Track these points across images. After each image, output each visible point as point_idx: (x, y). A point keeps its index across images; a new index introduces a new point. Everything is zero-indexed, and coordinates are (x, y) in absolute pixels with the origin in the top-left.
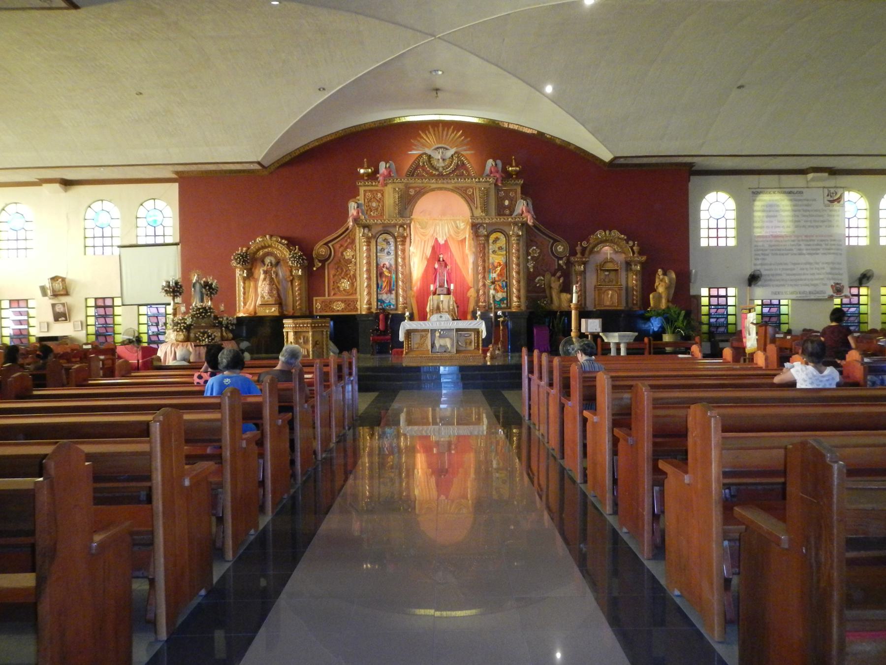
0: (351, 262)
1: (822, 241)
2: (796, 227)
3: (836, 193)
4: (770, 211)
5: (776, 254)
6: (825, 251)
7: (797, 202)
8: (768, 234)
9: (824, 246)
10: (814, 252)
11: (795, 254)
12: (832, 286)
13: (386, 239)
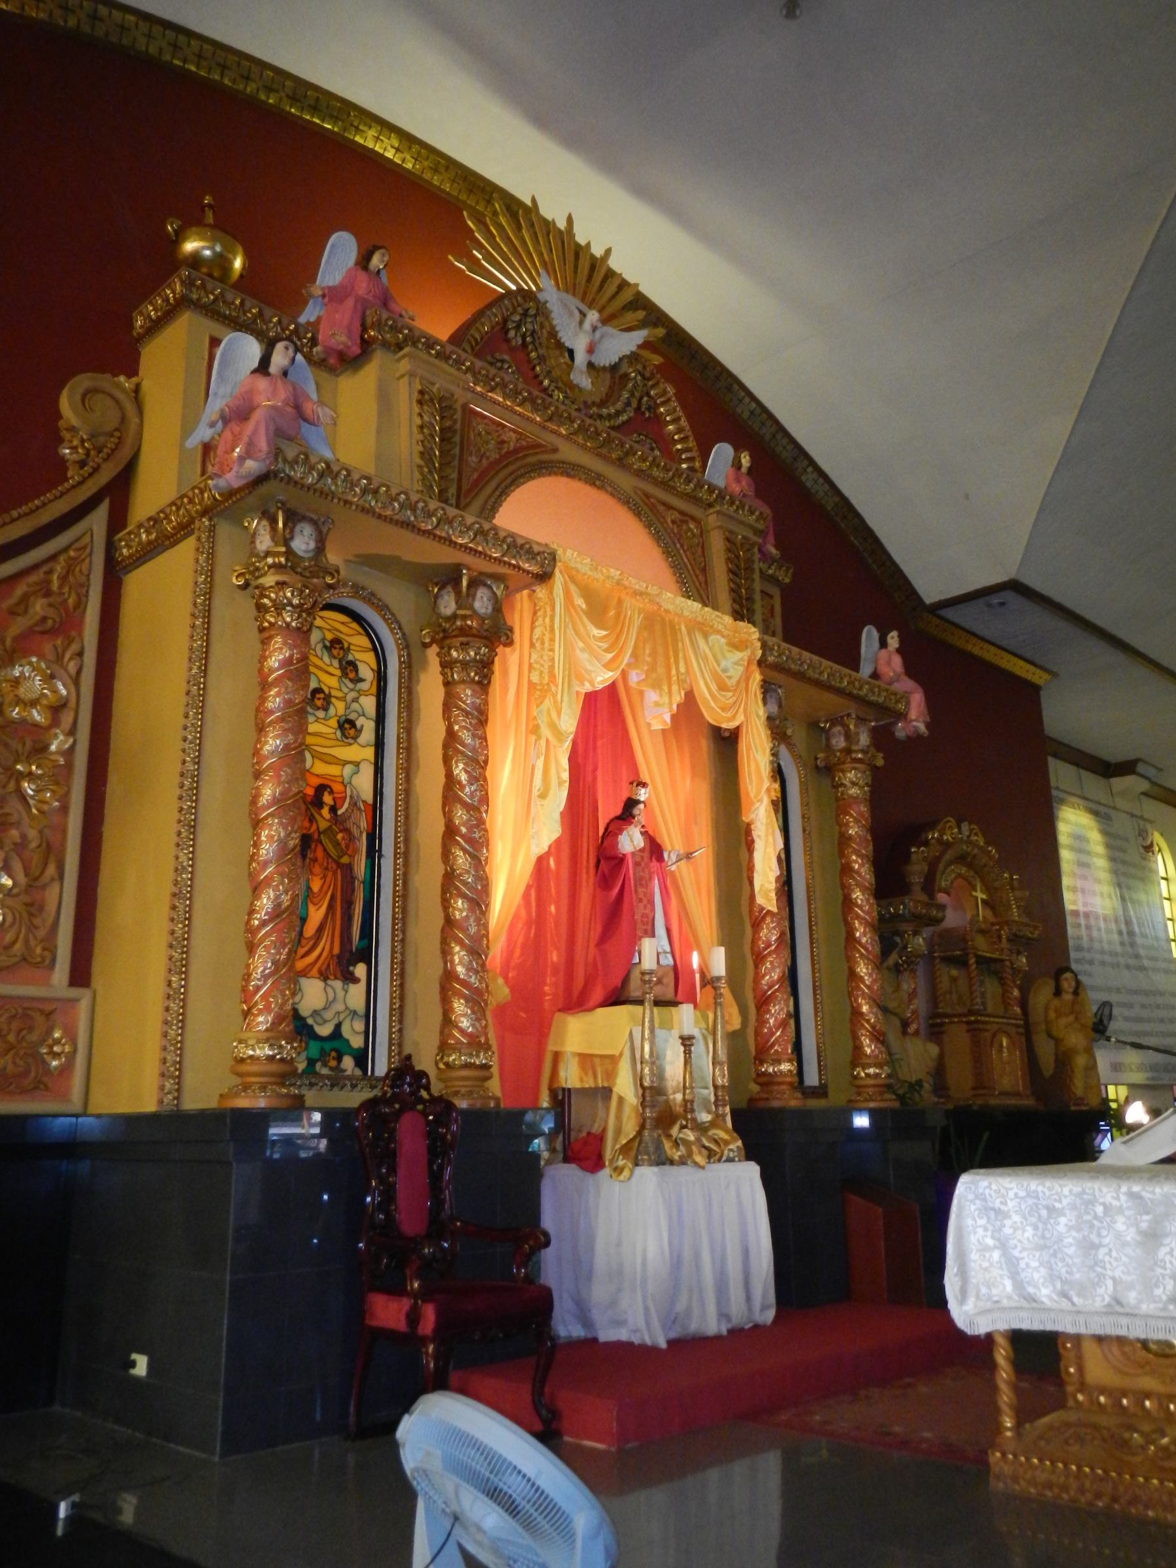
0: (40, 750)
13: (337, 642)
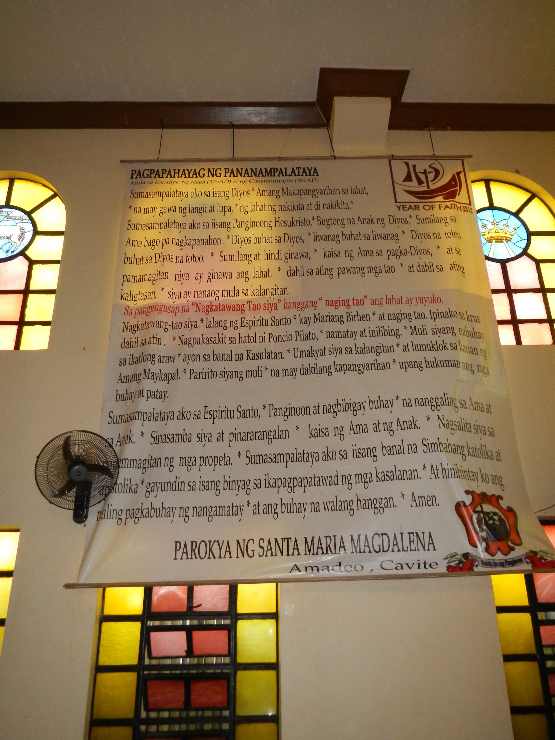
1: (397, 317)
2: (291, 273)
3: (437, 173)
4: (193, 226)
5: (211, 374)
6: (418, 356)
7: (295, 199)
8: (182, 301)
9: (406, 337)
10: (369, 358)
11: (290, 372)
12: (458, 507)
